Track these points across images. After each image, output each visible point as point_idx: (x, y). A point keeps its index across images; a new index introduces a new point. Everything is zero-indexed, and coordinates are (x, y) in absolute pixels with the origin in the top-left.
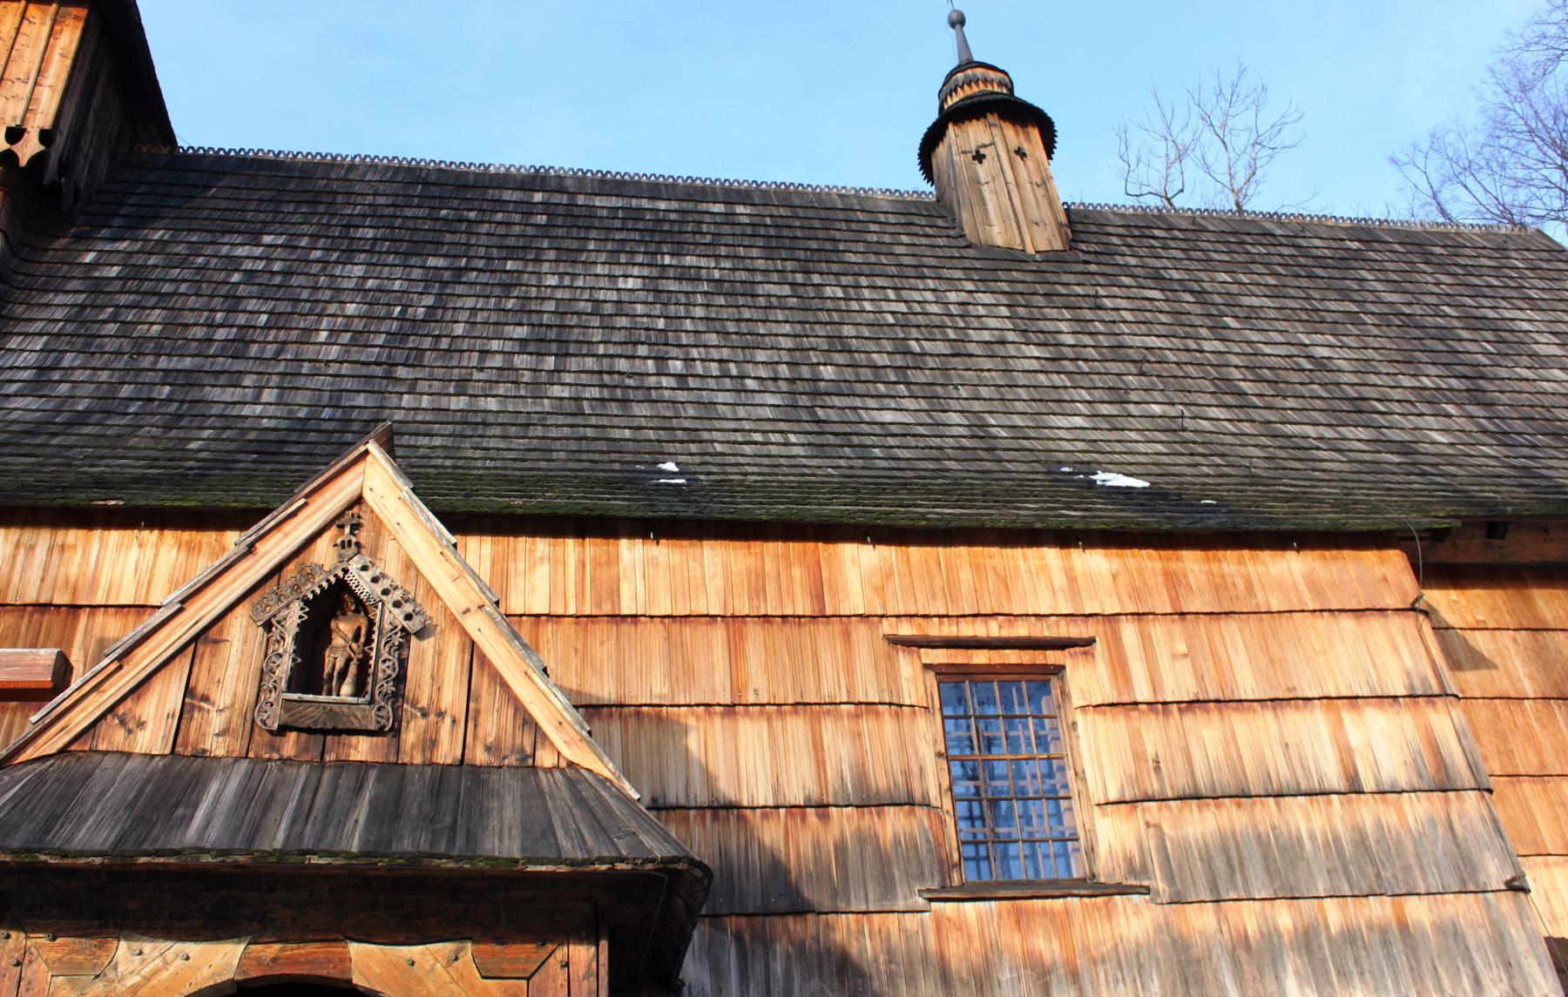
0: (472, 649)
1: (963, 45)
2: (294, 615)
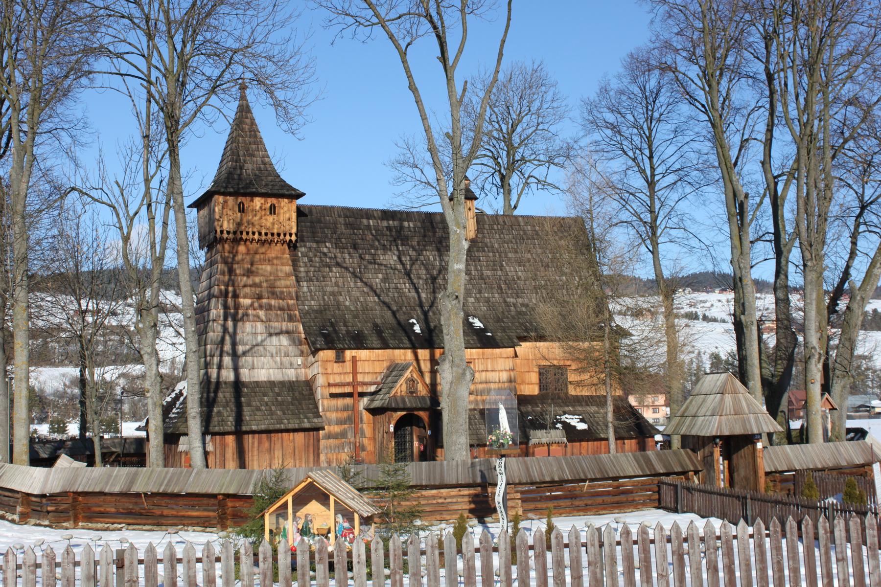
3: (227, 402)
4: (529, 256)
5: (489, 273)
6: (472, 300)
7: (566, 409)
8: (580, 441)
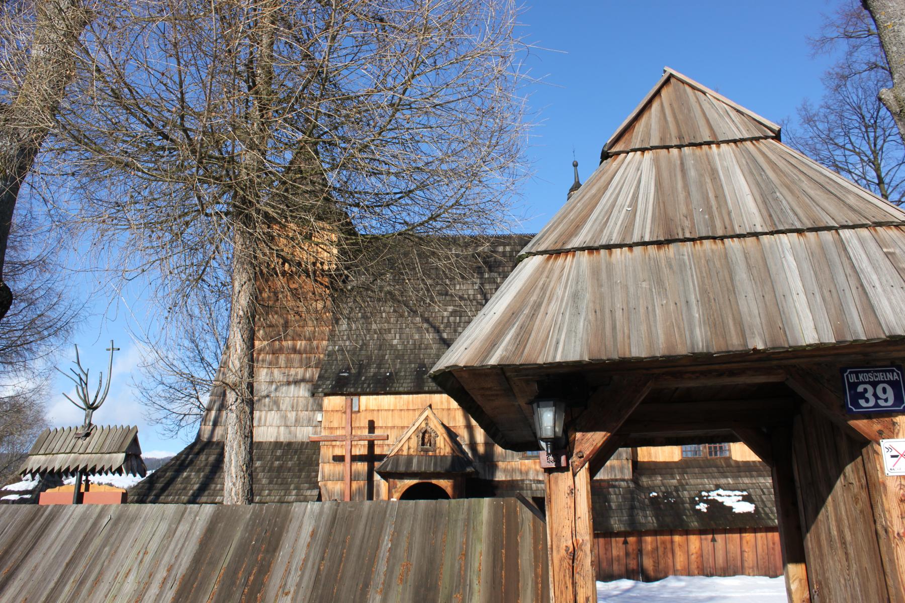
1: (577, 176)
2: (421, 435)
3: (206, 465)
7: (723, 481)
8: (741, 531)
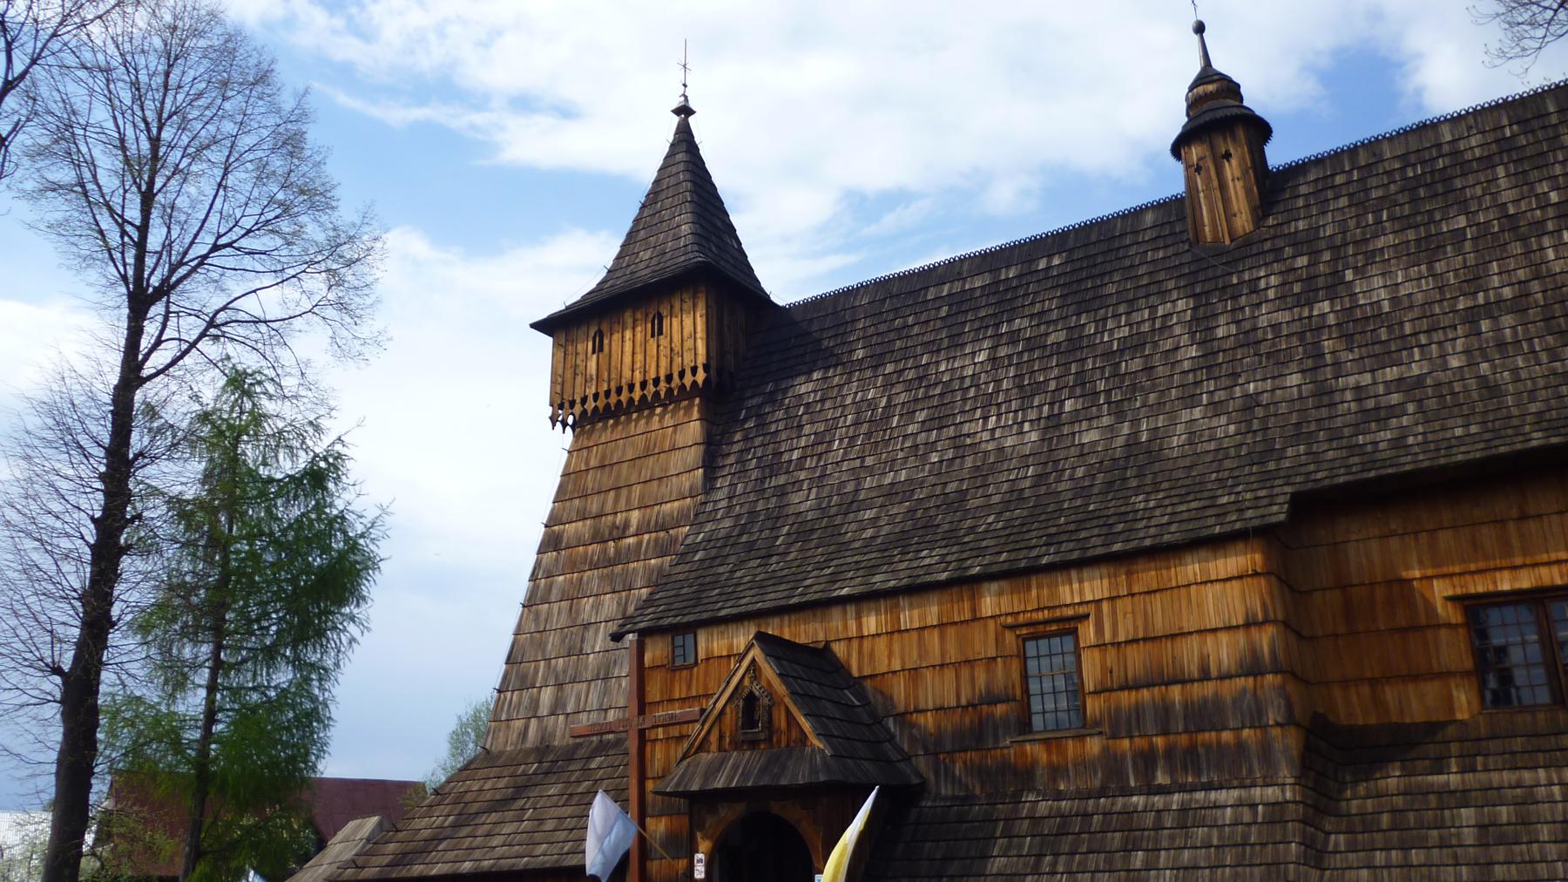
0: (787, 709)
4: (1462, 222)
5: (1283, 317)
6: (1197, 413)
